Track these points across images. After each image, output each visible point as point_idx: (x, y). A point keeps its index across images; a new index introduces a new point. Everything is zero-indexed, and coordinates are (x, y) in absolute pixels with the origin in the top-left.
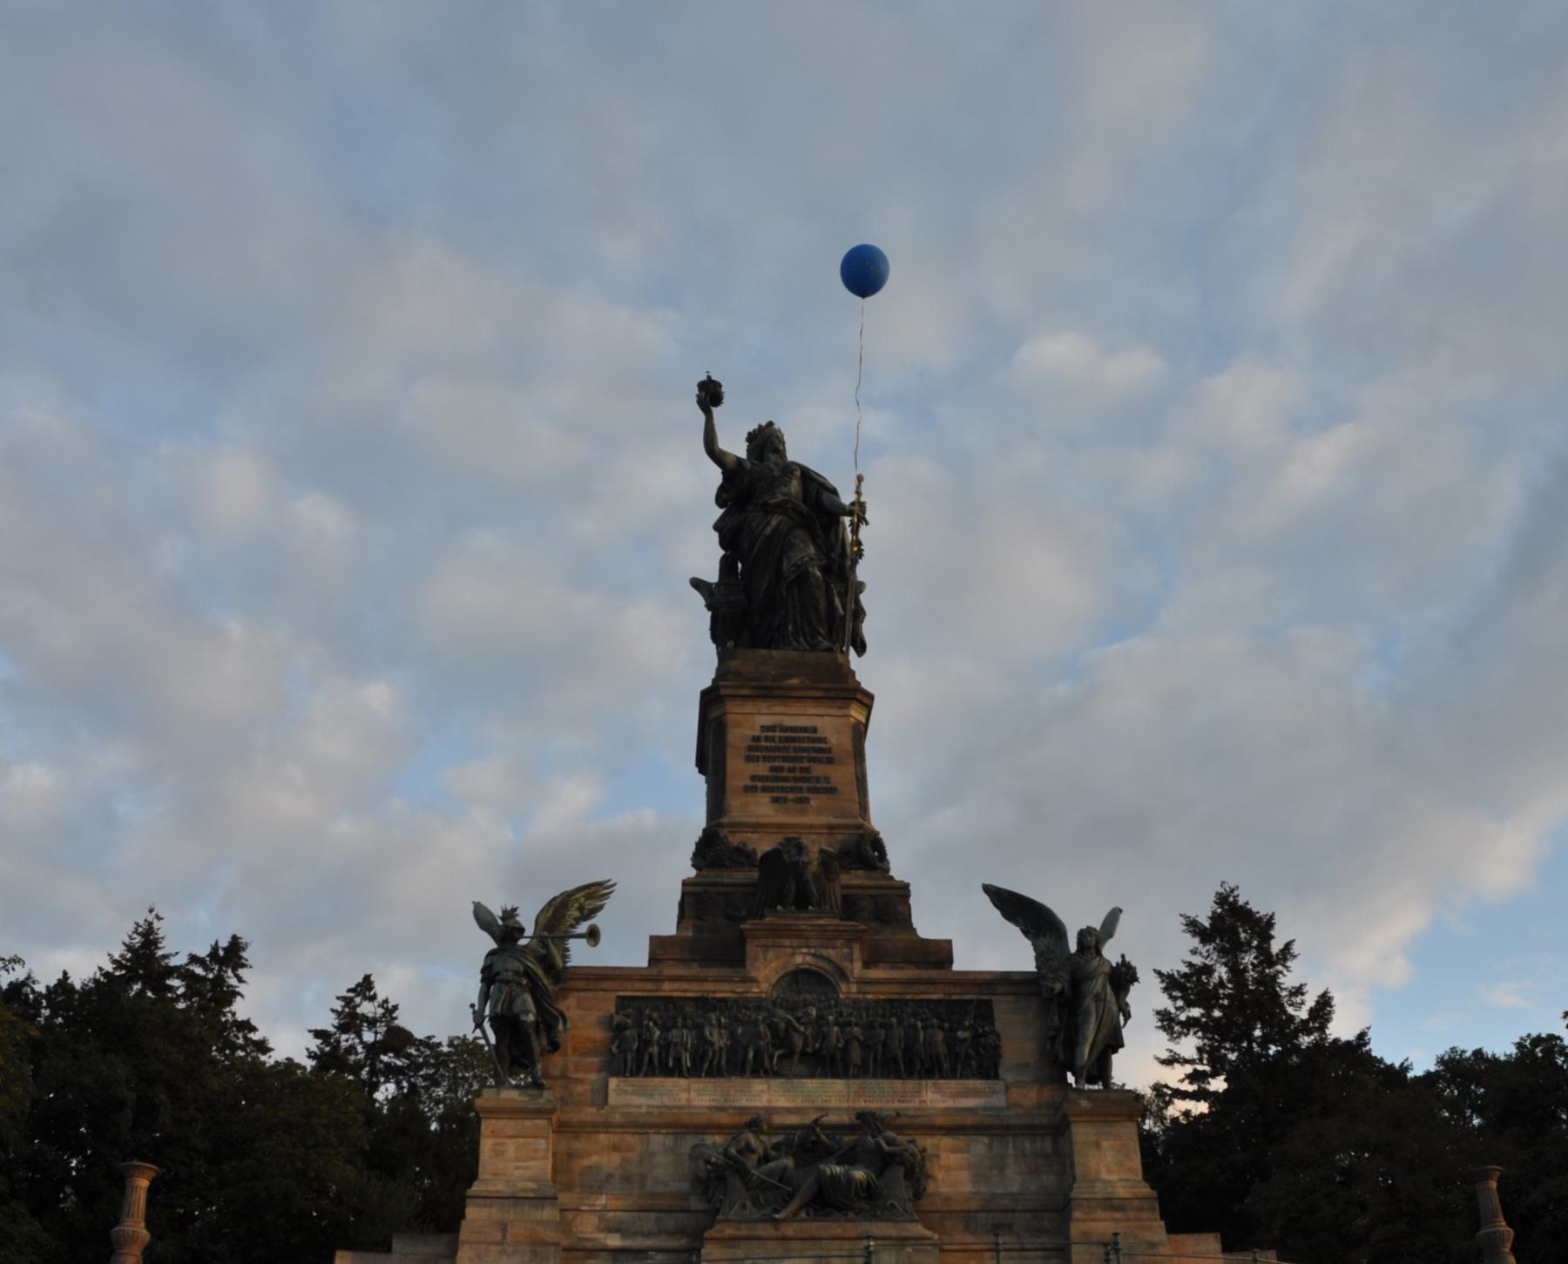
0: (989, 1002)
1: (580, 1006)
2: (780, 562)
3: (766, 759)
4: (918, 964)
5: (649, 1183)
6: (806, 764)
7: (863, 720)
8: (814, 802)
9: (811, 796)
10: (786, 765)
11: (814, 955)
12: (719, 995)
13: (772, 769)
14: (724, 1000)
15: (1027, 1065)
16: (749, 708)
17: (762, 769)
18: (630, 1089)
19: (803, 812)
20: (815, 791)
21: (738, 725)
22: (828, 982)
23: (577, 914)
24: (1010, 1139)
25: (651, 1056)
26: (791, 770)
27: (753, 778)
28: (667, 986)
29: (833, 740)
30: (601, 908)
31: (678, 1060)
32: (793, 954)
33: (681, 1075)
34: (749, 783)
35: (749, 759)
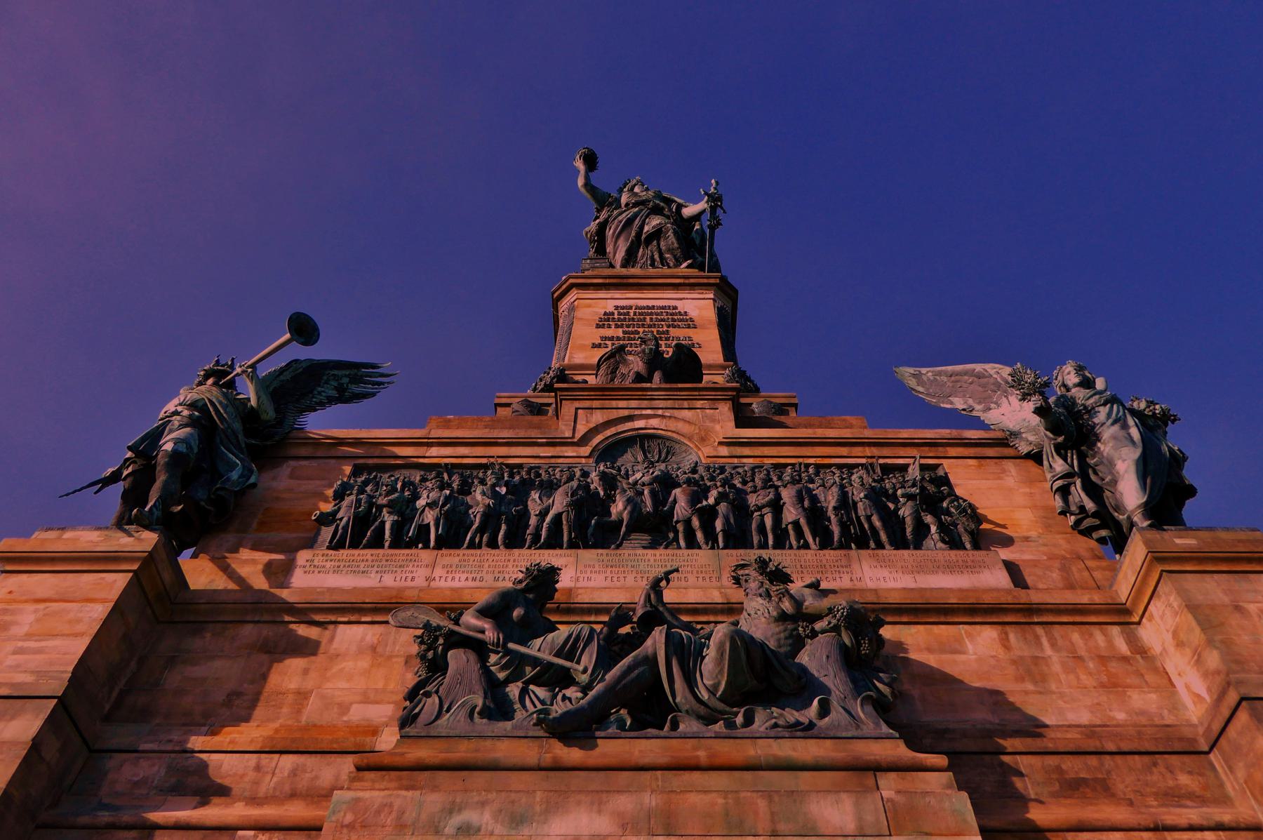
1: (292, 476)
2: (642, 227)
3: (617, 326)
5: (313, 703)
7: (729, 310)
10: (641, 330)
11: (663, 417)
14: (520, 466)
16: (602, 294)
18: (328, 564)
23: (334, 393)
24: (1040, 630)
25: (383, 523)
27: (602, 338)
28: (434, 451)
29: (693, 313)
30: (374, 395)
31: (424, 529)
32: (630, 418)
33: (426, 546)
34: (598, 341)
35: (598, 326)
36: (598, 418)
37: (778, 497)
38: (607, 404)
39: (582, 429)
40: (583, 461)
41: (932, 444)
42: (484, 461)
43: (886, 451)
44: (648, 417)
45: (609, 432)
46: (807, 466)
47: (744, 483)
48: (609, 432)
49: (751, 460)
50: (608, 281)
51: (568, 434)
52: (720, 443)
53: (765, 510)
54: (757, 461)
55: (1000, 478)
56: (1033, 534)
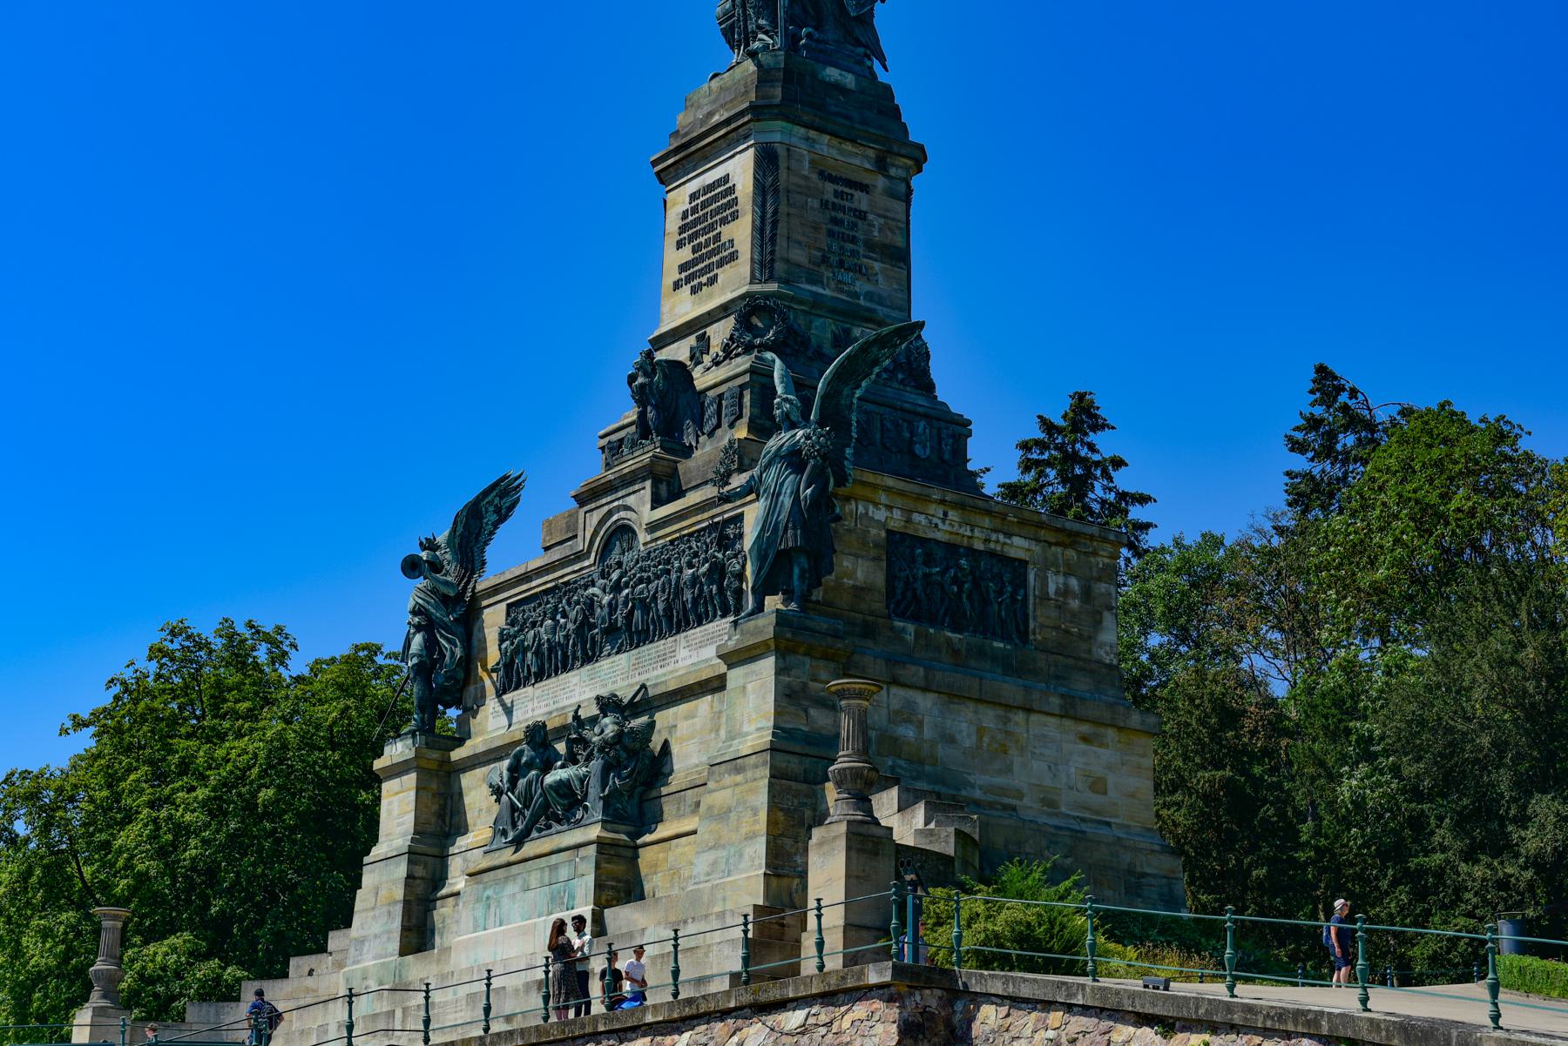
8: (724, 274)
19: (710, 296)
20: (721, 264)
26: (707, 244)
32: (610, 513)
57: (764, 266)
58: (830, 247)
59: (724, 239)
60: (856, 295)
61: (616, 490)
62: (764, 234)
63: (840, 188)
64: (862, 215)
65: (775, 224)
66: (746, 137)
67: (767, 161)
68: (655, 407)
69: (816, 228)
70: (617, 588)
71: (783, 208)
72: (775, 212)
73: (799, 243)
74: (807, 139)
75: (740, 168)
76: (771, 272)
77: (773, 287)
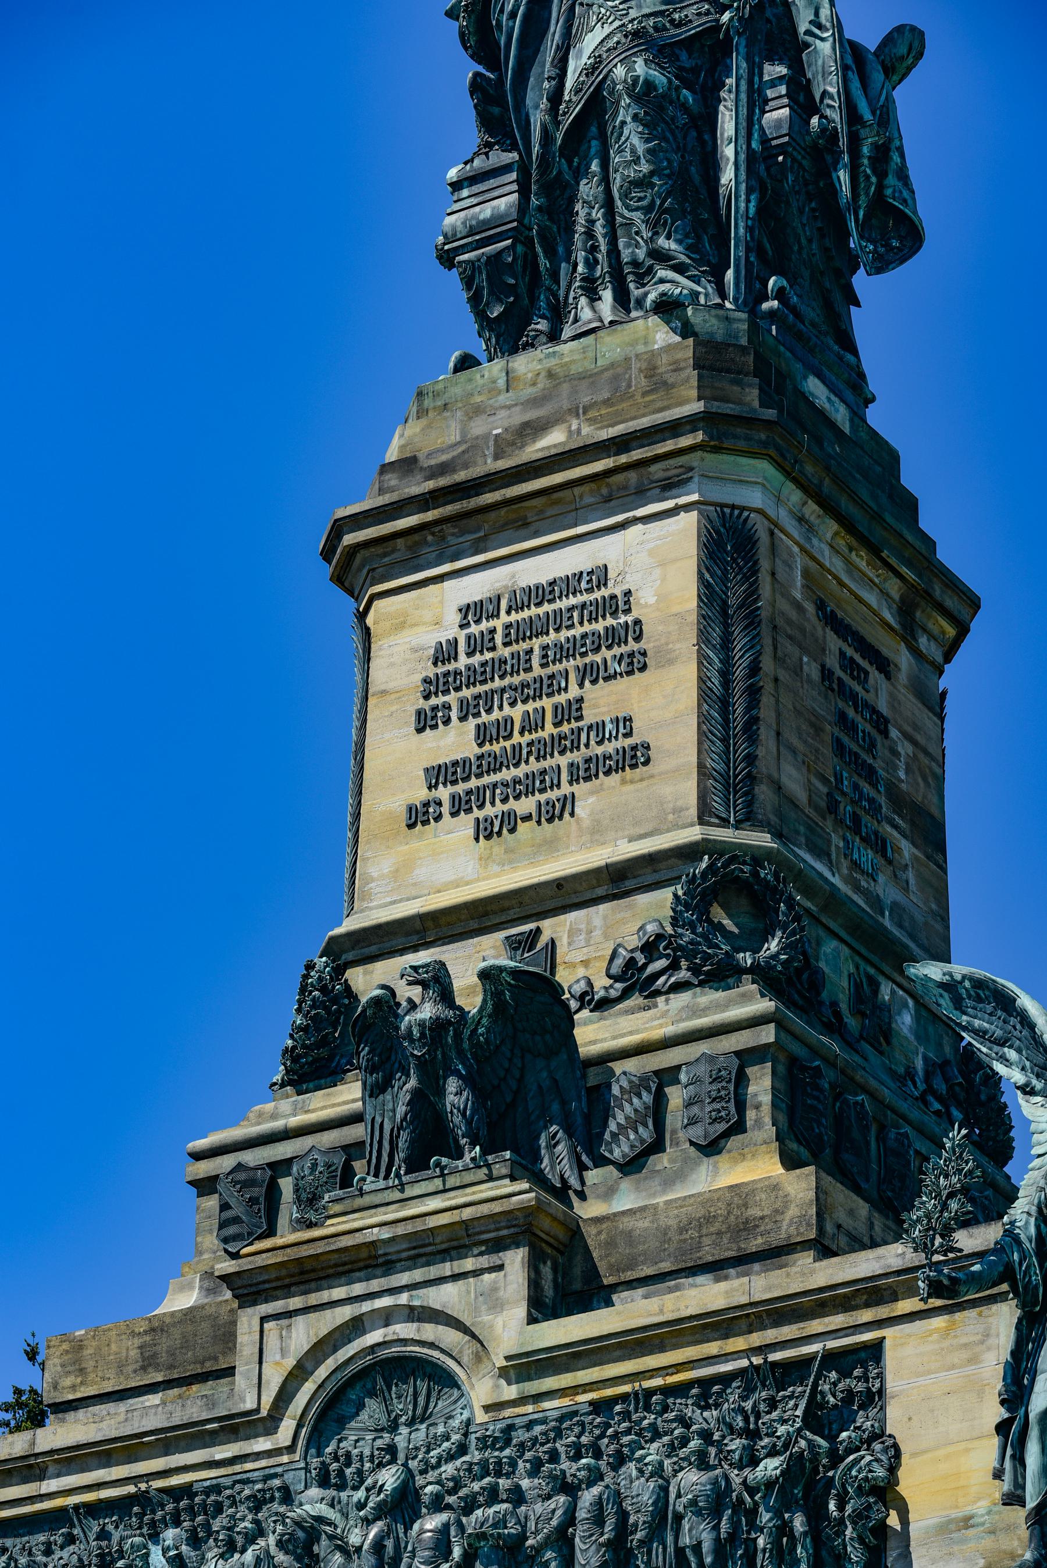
0: (876, 1349)
4: (716, 1268)
6: (574, 692)
8: (591, 800)
9: (580, 789)
10: (517, 713)
12: (175, 1481)
13: (483, 735)
14: (186, 1490)
15: (967, 1522)
17: (456, 741)
19: (551, 847)
20: (586, 772)
21: (401, 626)
22: (450, 1381)
26: (530, 724)
27: (437, 775)
32: (356, 1326)
34: (421, 794)
35: (425, 722)
36: (303, 1334)
37: (570, 1519)
38: (314, 1299)
39: (274, 1379)
40: (285, 1459)
41: (874, 1292)
42: (131, 1489)
43: (788, 1332)
44: (387, 1317)
45: (322, 1372)
46: (649, 1393)
47: (535, 1469)
48: (322, 1372)
49: (556, 1403)
50: (430, 515)
51: (250, 1404)
52: (503, 1373)
53: (549, 1555)
54: (566, 1402)
55: (974, 1360)
56: (980, 1507)
57: (731, 780)
58: (839, 779)
59: (590, 716)
60: (876, 903)
61: (389, 1267)
62: (729, 712)
63: (850, 652)
64: (881, 724)
65: (753, 693)
66: (669, 486)
67: (729, 549)
68: (468, 1081)
69: (818, 730)
70: (404, 1505)
71: (767, 664)
72: (754, 669)
73: (794, 751)
74: (801, 520)
75: (655, 560)
76: (749, 804)
77: (762, 839)
